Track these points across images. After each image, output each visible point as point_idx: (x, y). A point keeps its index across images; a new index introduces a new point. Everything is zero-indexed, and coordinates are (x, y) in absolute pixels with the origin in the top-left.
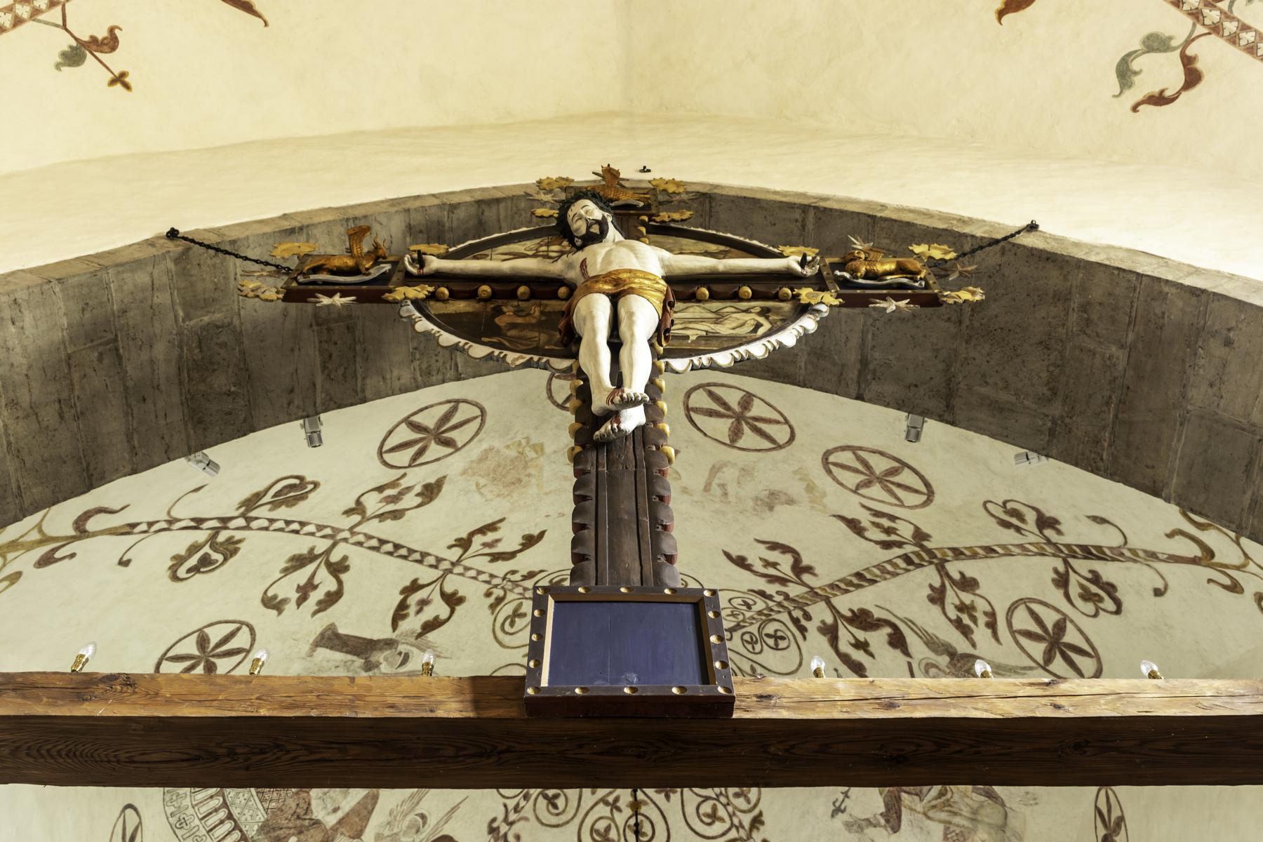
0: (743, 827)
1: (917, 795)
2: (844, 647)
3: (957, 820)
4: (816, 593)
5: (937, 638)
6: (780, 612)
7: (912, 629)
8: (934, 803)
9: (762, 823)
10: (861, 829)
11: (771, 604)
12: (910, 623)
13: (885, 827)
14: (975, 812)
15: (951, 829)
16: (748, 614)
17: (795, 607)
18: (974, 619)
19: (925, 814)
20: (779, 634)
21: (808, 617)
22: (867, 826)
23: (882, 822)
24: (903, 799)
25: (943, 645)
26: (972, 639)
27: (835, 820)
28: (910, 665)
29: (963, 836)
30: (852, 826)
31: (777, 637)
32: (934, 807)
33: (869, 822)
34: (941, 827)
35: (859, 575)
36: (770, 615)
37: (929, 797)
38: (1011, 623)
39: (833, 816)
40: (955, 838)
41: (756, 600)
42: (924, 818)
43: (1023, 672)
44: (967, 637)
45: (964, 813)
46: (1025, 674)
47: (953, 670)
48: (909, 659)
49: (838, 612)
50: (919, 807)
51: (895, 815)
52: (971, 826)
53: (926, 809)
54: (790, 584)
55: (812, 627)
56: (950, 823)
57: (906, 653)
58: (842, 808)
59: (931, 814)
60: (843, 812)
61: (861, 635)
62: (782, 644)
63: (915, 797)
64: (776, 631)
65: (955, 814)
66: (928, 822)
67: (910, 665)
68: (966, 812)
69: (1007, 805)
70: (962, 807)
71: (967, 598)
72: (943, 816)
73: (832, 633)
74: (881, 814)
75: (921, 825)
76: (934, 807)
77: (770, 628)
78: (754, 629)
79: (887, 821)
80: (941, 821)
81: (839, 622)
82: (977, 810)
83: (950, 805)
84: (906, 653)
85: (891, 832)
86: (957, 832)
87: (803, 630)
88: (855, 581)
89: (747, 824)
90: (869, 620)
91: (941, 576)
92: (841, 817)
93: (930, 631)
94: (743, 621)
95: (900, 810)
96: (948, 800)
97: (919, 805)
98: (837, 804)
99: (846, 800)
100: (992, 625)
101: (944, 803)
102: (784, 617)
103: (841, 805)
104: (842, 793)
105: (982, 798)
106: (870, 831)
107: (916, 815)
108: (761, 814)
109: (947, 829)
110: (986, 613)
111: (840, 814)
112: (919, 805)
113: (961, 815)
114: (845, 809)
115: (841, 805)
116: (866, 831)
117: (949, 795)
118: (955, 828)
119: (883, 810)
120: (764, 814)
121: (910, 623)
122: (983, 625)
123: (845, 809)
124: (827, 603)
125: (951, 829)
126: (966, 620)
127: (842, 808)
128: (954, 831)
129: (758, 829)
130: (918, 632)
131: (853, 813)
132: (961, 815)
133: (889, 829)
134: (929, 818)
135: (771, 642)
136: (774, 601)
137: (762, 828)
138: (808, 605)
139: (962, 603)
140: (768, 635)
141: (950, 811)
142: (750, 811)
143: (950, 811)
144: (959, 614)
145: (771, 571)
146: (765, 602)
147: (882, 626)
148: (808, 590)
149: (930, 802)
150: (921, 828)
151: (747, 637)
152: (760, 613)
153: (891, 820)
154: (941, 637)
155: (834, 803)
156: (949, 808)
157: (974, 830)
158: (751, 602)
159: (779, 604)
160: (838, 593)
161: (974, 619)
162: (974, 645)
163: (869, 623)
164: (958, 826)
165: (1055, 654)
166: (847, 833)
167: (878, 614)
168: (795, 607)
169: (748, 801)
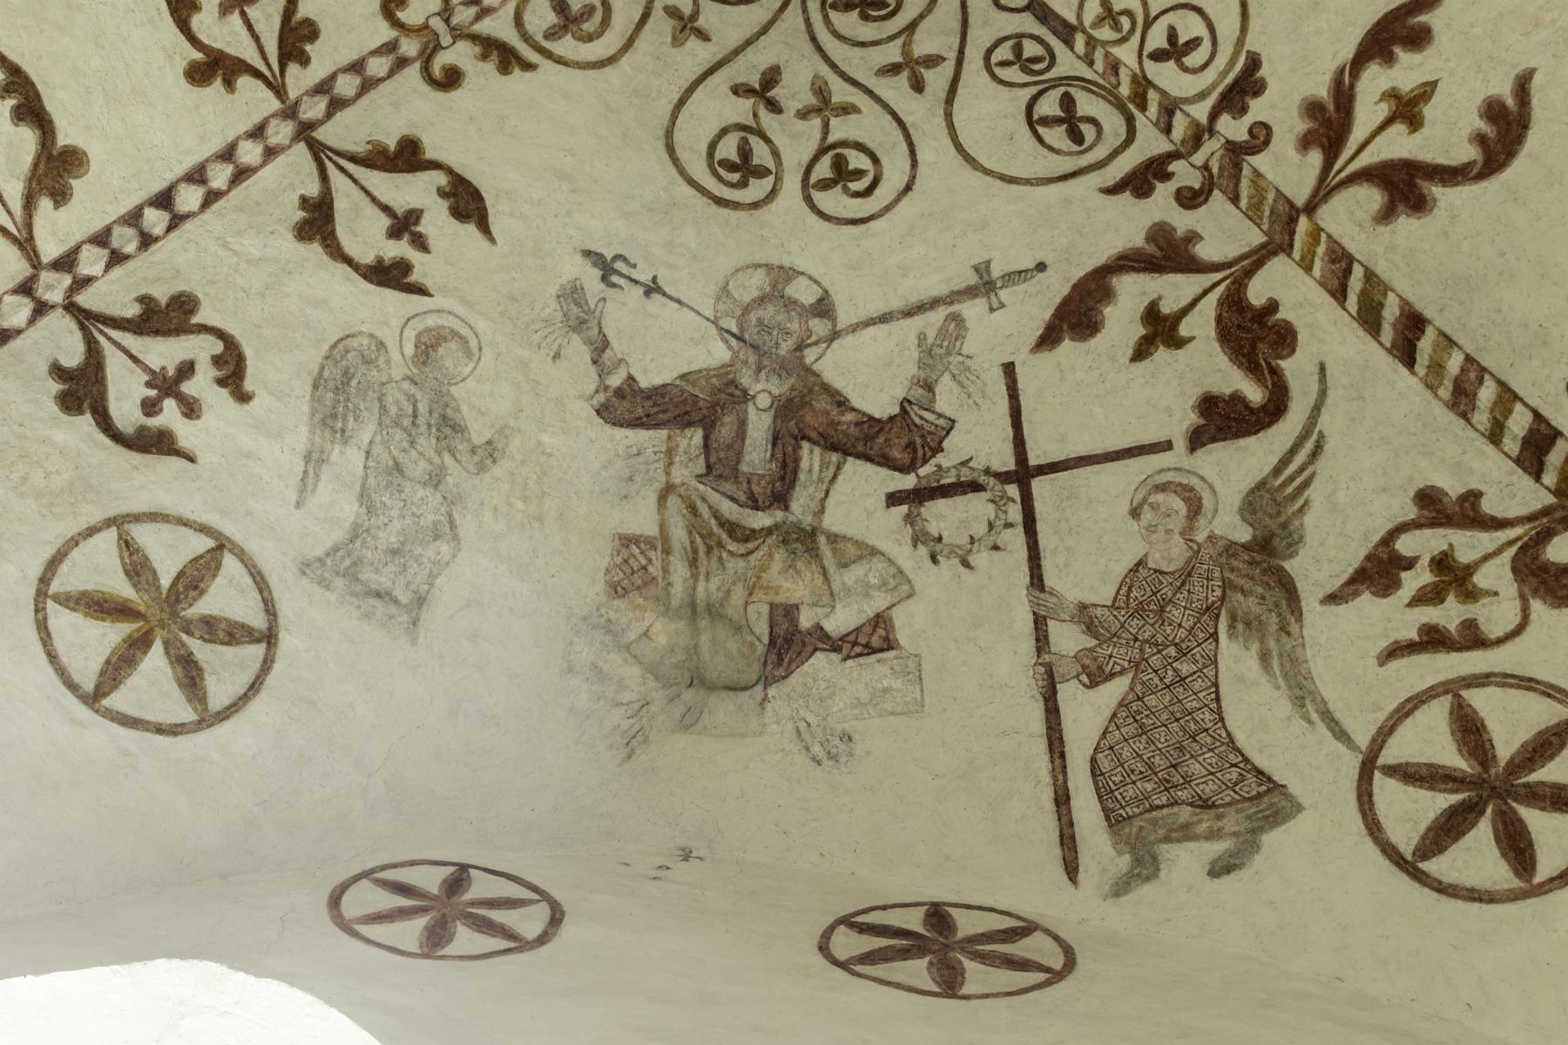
0: (478, 18)
1: (709, 467)
2: (1133, 292)
3: (679, 570)
4: (1292, 221)
5: (1301, 510)
6: (1168, 130)
7: (1293, 451)
8: (704, 511)
9: (504, 68)
10: (579, 326)
11: (1201, 111)
12: (1312, 443)
13: (1421, 379)
14: (714, 612)
15: (652, 554)
16: (1126, 54)
17: (1206, 167)
18: (1429, 596)
19: (668, 490)
20: (1088, 131)
21: (1190, 199)
22: (589, 342)
23: (615, 381)
24: (688, 432)
25: (1285, 526)
26: (1356, 594)
27: (578, 258)
28: (1167, 446)
29: (646, 584)
30: (577, 304)
31: (1070, 121)
32: (694, 510)
33: (600, 347)
34: (651, 530)
35: (1414, 323)
36: (1143, 107)
37: (714, 498)
38: (1484, 685)
39: (587, 253)
40: (635, 566)
41: (1210, 75)
42: (658, 485)
43: (1315, 716)
44: (1352, 581)
45: (701, 585)
46: (1310, 722)
47: (1206, 553)
48: (1180, 444)
49: (1249, 273)
50: (680, 474)
51: (640, 412)
52: (675, 603)
53: (682, 490)
54: (1315, 158)
55: (1161, 205)
56: (667, 551)
57: (1197, 440)
58: (615, 279)
59: (673, 502)
60: (604, 278)
61: (1201, 325)
62: (1056, 136)
63: (701, 462)
64: (1093, 121)
65: (693, 563)
66: (652, 500)
67: (1167, 446)
68: (707, 589)
69: (772, 691)
70: (714, 584)
71: (1496, 576)
72: (679, 534)
73: (1166, 258)
74: (631, 378)
75: (638, 478)
76: (694, 510)
77: (1087, 105)
78: (1067, 63)
79: (619, 393)
80: (662, 526)
81: (1218, 276)
82: (722, 617)
83: (709, 550)
84: (1197, 440)
85: (595, 402)
86: (651, 569)
87: (1141, 182)
88: (1391, 311)
89: (486, 27)
90: (1262, 347)
91: (1531, 518)
92: (591, 277)
93: (1315, 493)
94: (1092, 43)
95: (657, 426)
96: (721, 545)
97: (686, 472)
98: (619, 265)
99: (641, 290)
100: (1433, 640)
101: (711, 534)
102: (1150, 143)
103: (622, 275)
104: (654, 279)
105: (763, 629)
106: (578, 351)
107: (661, 465)
108: (528, 66)
109: (650, 542)
110: (1470, 625)
111: (598, 273)
112: (686, 472)
113: (695, 577)
114: (614, 286)
115: (622, 275)
116: (575, 338)
117: (733, 546)
118: (658, 564)
119: (644, 382)
120: (528, 75)
121: (1309, 446)
122: (1425, 620)
123: (614, 286)
124: (1263, 246)
125: (652, 554)
126: (1413, 581)
127: (615, 279)
128: (650, 560)
129: (484, 57)
130: (1292, 467)
131: (609, 306)
132: (695, 577)
133: (601, 397)
134: (663, 498)
135: (1049, 106)
136: (1214, 116)
137: (490, 67)
138: (1235, 199)
139: (1470, 569)
140: (1068, 102)
141: (695, 551)
142: (526, 38)
143: (695, 551)
144: (1425, 560)
145: (1368, 112)
146: (1202, 96)
147: (1260, 379)
148: (1300, 200)
149: (704, 500)
150: (631, 479)
151: (1031, 49)
152: (1142, 85)
153: (626, 404)
154: (1309, 520)
155: (617, 257)
156: (702, 550)
157: (667, 611)
158: (1195, 59)
159: (1197, 137)
160: (1317, 271)
161: (1429, 596)
162: (1332, 599)
163: (1254, 348)
164: (666, 570)
165: (1451, 791)
166: (554, 289)
167: (1296, 369)
168: (1206, 167)
169: (551, 35)
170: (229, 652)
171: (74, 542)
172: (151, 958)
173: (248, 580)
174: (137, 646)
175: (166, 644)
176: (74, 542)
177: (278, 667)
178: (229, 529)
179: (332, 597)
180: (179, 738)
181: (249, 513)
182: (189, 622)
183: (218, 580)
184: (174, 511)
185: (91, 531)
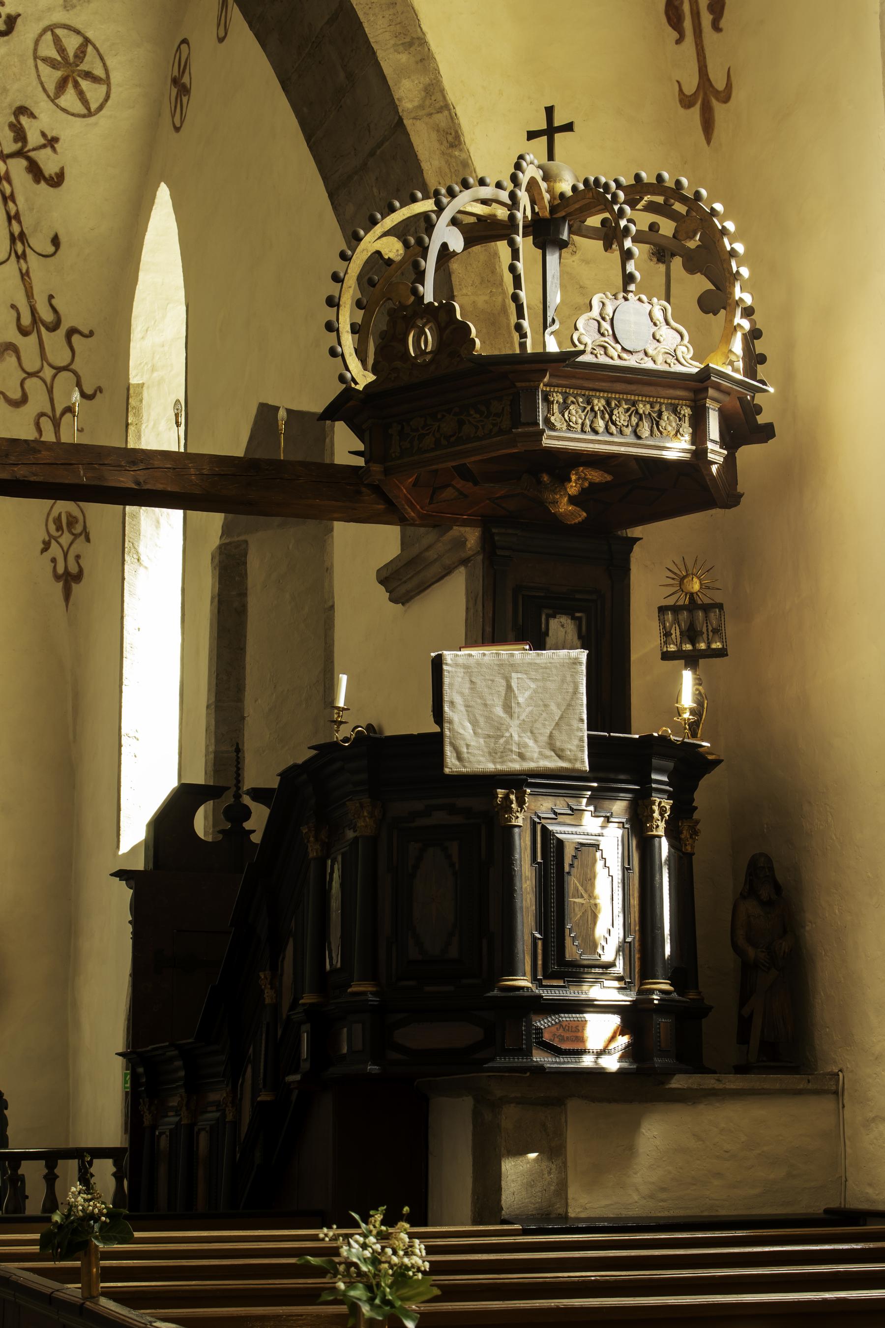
170: (87, 59)
171: (39, 76)
172: (156, 195)
173: (66, 31)
174: (76, 85)
175: (79, 76)
176: (39, 76)
177: (98, 45)
178: (46, 23)
179: (78, 8)
180: (111, 95)
181: (43, 11)
182: (74, 62)
183: (63, 40)
184: (36, 36)
185: (36, 67)
